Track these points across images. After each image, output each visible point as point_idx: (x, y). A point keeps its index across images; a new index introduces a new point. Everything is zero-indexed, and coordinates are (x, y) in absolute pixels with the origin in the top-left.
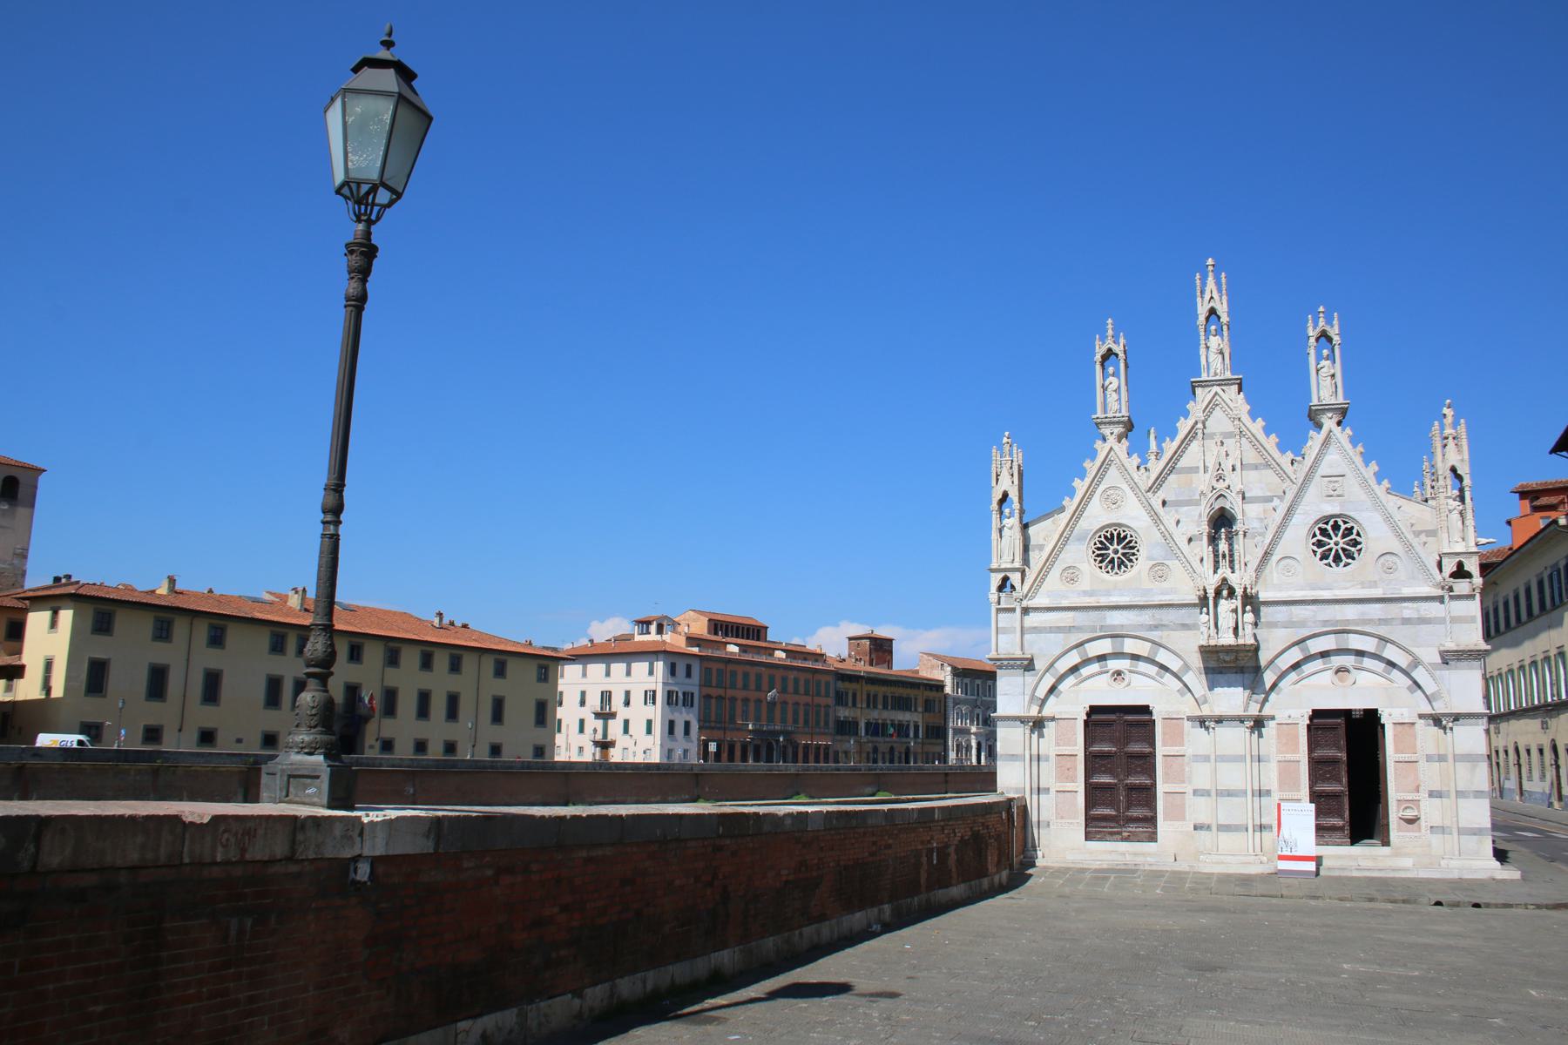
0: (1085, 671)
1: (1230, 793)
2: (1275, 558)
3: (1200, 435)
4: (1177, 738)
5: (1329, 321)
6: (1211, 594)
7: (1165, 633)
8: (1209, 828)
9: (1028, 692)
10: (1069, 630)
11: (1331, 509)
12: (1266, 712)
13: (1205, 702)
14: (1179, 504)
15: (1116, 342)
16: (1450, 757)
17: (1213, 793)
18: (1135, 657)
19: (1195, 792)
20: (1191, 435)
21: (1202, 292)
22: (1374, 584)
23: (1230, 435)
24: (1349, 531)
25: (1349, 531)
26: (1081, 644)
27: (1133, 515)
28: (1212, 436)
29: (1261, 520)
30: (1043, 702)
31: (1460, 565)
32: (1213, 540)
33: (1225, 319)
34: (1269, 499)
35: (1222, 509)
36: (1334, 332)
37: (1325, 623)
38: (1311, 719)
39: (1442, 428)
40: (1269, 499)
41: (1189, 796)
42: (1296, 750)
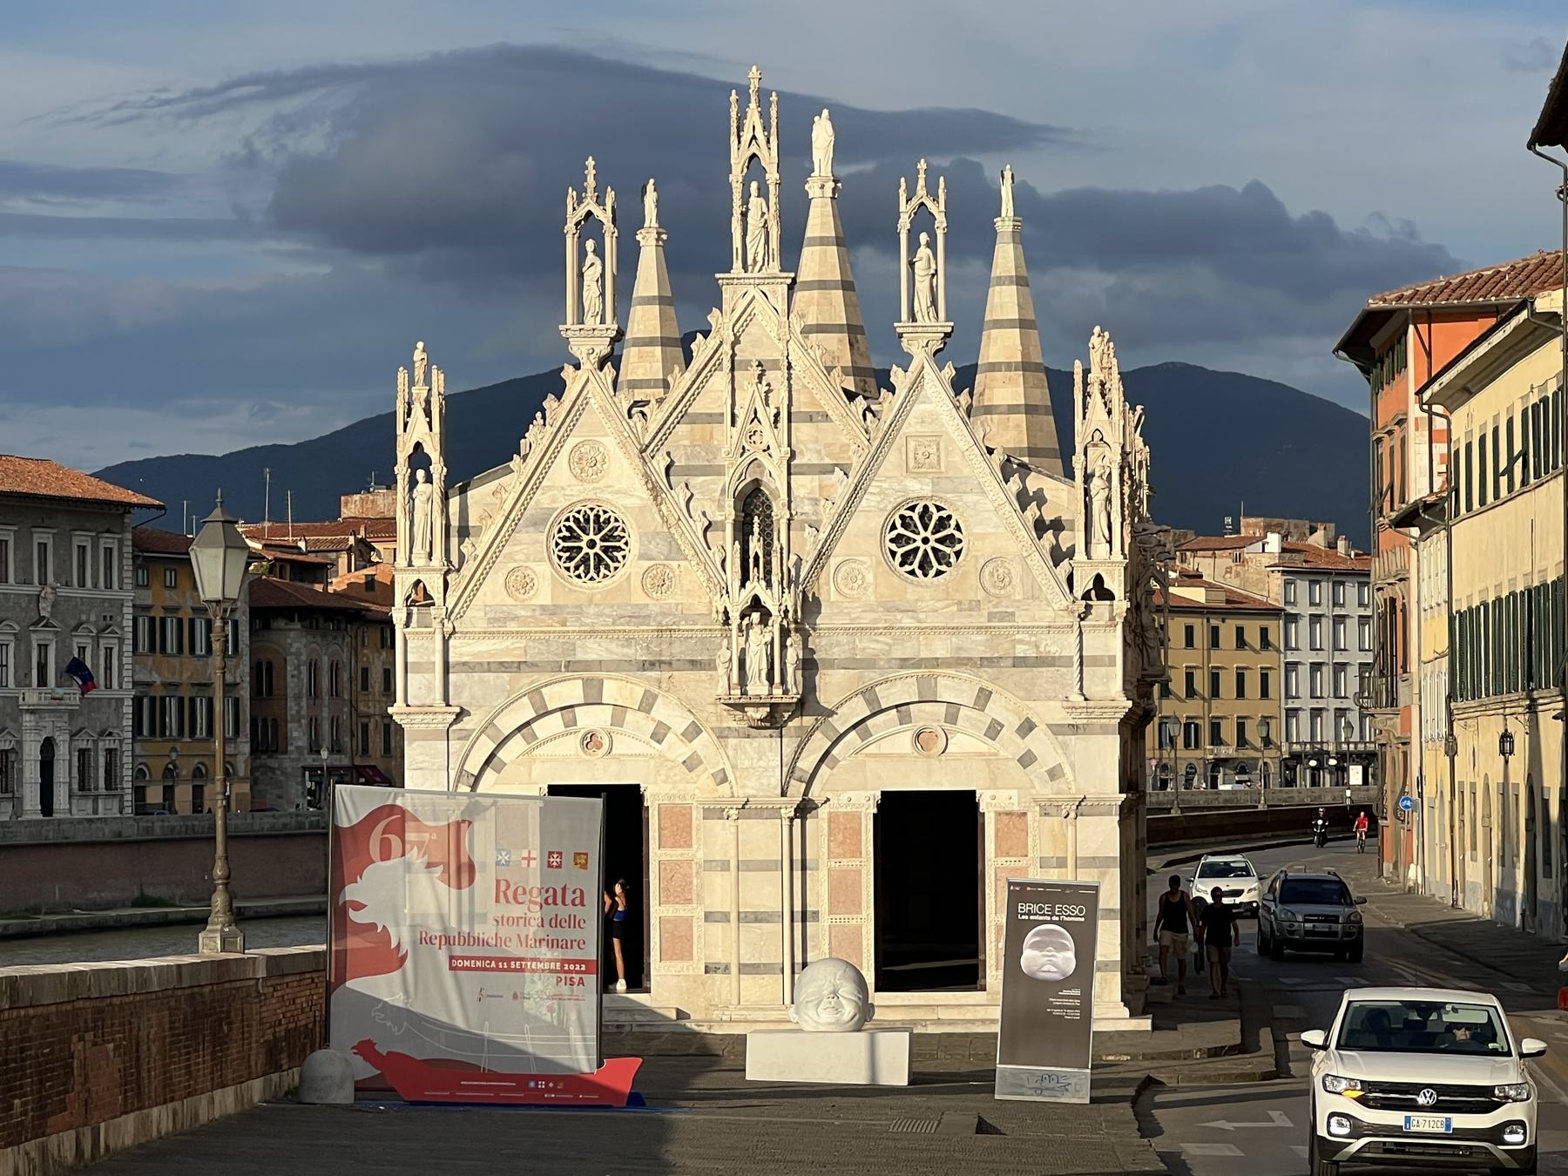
0: (542, 728)
1: (758, 918)
2: (833, 562)
3: (727, 364)
4: (681, 833)
5: (932, 192)
6: (735, 616)
7: (666, 674)
8: (727, 969)
9: (454, 766)
10: (519, 666)
11: (919, 489)
12: (816, 794)
13: (725, 779)
14: (691, 471)
15: (600, 201)
16: (1070, 862)
17: (733, 917)
18: (619, 710)
19: (708, 917)
20: (713, 364)
21: (740, 129)
22: (975, 605)
23: (775, 365)
24: (943, 523)
25: (943, 523)
26: (538, 690)
27: (621, 489)
28: (746, 365)
29: (815, 502)
30: (478, 778)
31: (1098, 580)
32: (743, 531)
33: (772, 176)
34: (827, 470)
35: (757, 482)
36: (938, 210)
37: (904, 663)
38: (878, 806)
39: (1086, 372)
40: (827, 470)
41: (699, 928)
42: (857, 853)
